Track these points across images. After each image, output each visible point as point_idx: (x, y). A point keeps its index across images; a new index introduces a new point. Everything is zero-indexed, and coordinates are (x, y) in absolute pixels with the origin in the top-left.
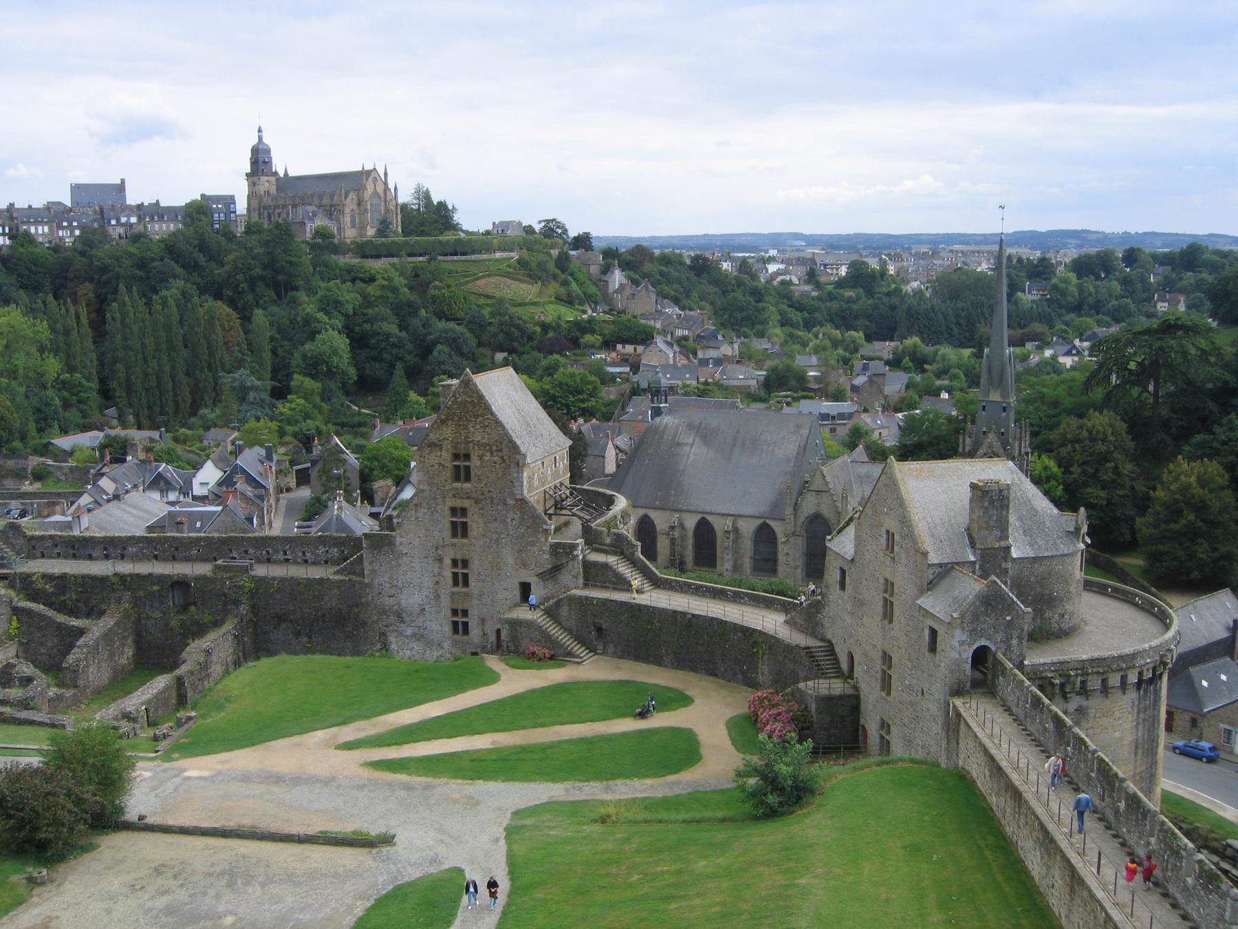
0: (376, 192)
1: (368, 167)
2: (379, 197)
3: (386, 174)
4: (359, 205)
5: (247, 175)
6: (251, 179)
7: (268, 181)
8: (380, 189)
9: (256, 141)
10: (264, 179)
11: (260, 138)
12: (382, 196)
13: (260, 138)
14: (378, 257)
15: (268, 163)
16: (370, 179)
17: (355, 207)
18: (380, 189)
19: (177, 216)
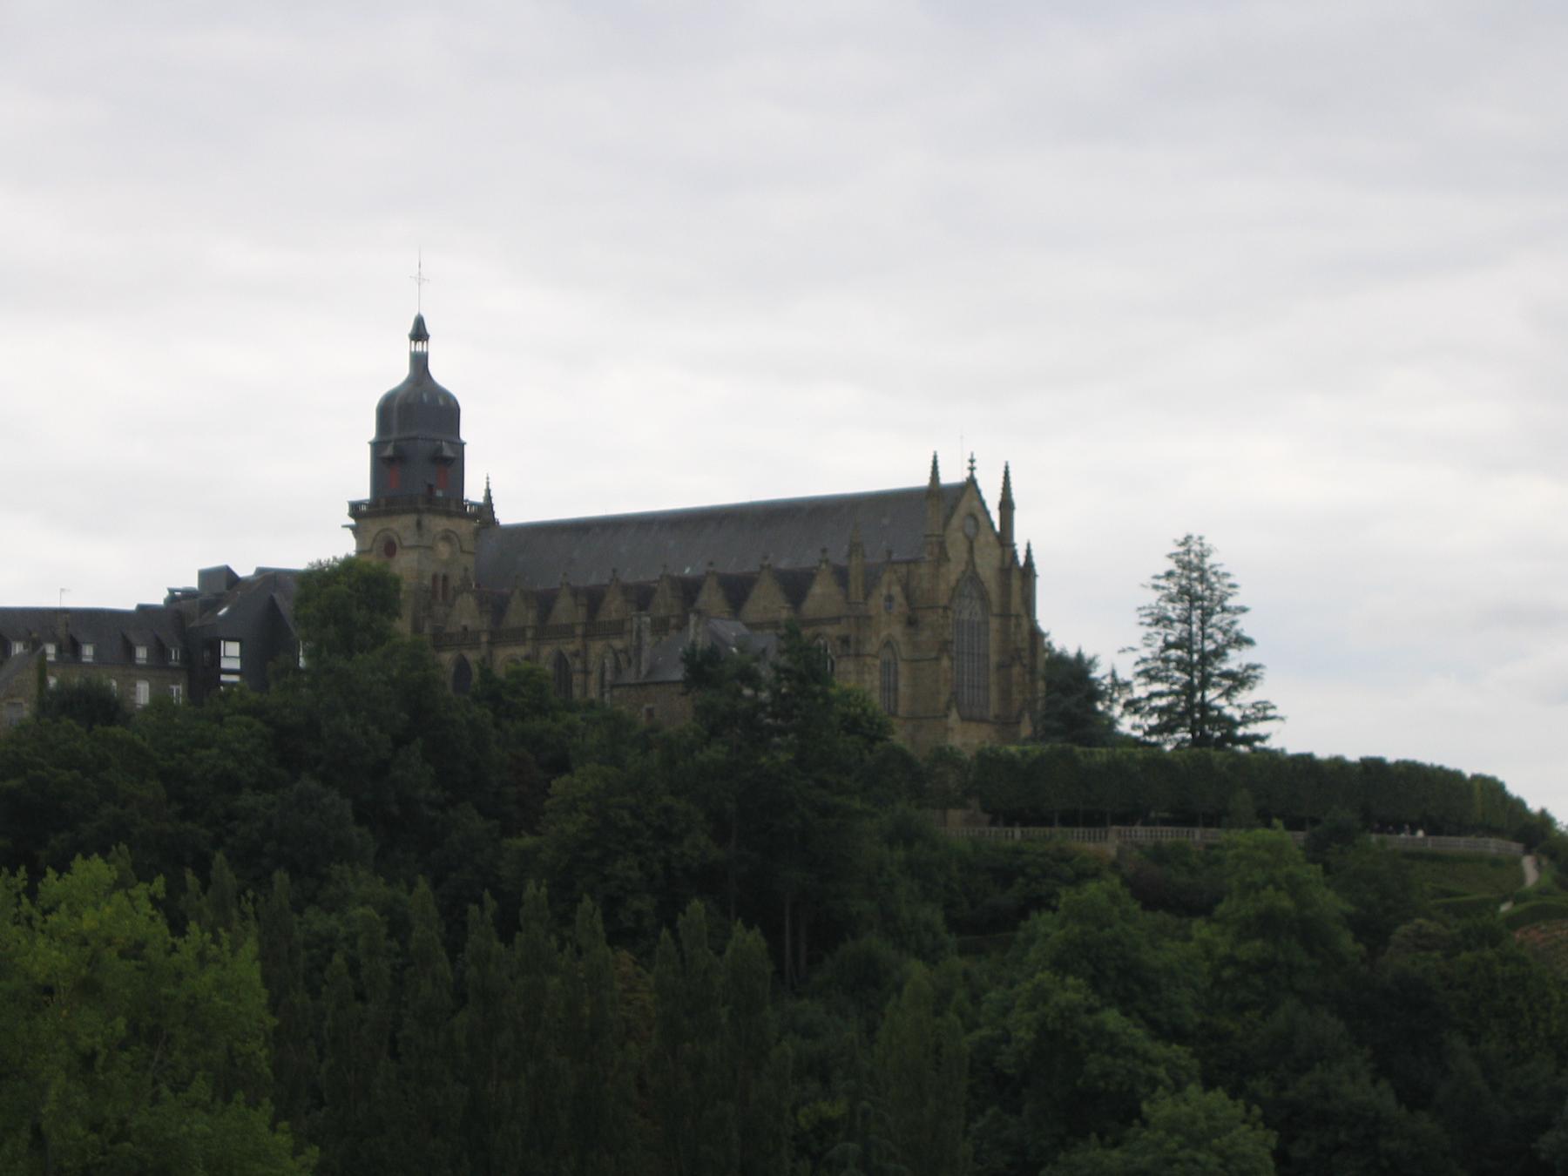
0: (972, 577)
1: (952, 475)
2: (984, 597)
3: (1007, 505)
4: (912, 622)
5: (355, 509)
6: (375, 527)
7: (447, 537)
8: (987, 566)
9: (397, 373)
10: (439, 524)
11: (420, 363)
12: (993, 587)
13: (420, 363)
14: (1093, 819)
15: (450, 462)
16: (956, 521)
17: (897, 631)
18: (987, 566)
19: (129, 650)
